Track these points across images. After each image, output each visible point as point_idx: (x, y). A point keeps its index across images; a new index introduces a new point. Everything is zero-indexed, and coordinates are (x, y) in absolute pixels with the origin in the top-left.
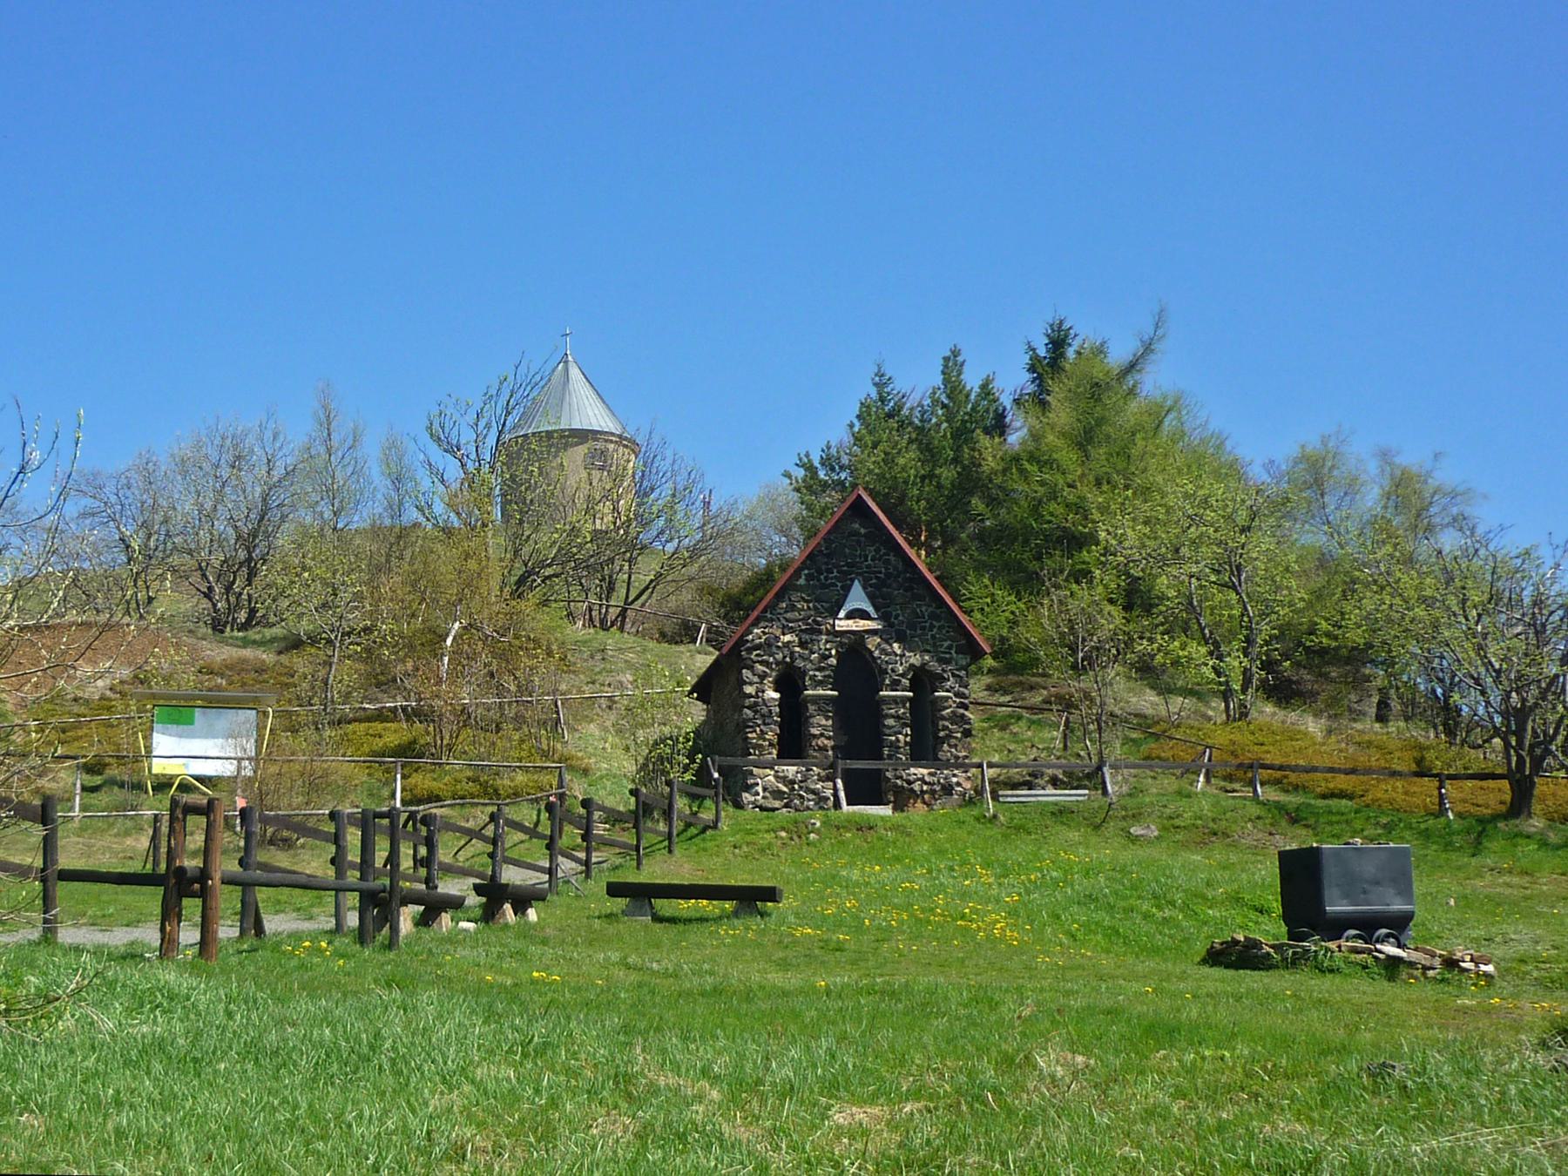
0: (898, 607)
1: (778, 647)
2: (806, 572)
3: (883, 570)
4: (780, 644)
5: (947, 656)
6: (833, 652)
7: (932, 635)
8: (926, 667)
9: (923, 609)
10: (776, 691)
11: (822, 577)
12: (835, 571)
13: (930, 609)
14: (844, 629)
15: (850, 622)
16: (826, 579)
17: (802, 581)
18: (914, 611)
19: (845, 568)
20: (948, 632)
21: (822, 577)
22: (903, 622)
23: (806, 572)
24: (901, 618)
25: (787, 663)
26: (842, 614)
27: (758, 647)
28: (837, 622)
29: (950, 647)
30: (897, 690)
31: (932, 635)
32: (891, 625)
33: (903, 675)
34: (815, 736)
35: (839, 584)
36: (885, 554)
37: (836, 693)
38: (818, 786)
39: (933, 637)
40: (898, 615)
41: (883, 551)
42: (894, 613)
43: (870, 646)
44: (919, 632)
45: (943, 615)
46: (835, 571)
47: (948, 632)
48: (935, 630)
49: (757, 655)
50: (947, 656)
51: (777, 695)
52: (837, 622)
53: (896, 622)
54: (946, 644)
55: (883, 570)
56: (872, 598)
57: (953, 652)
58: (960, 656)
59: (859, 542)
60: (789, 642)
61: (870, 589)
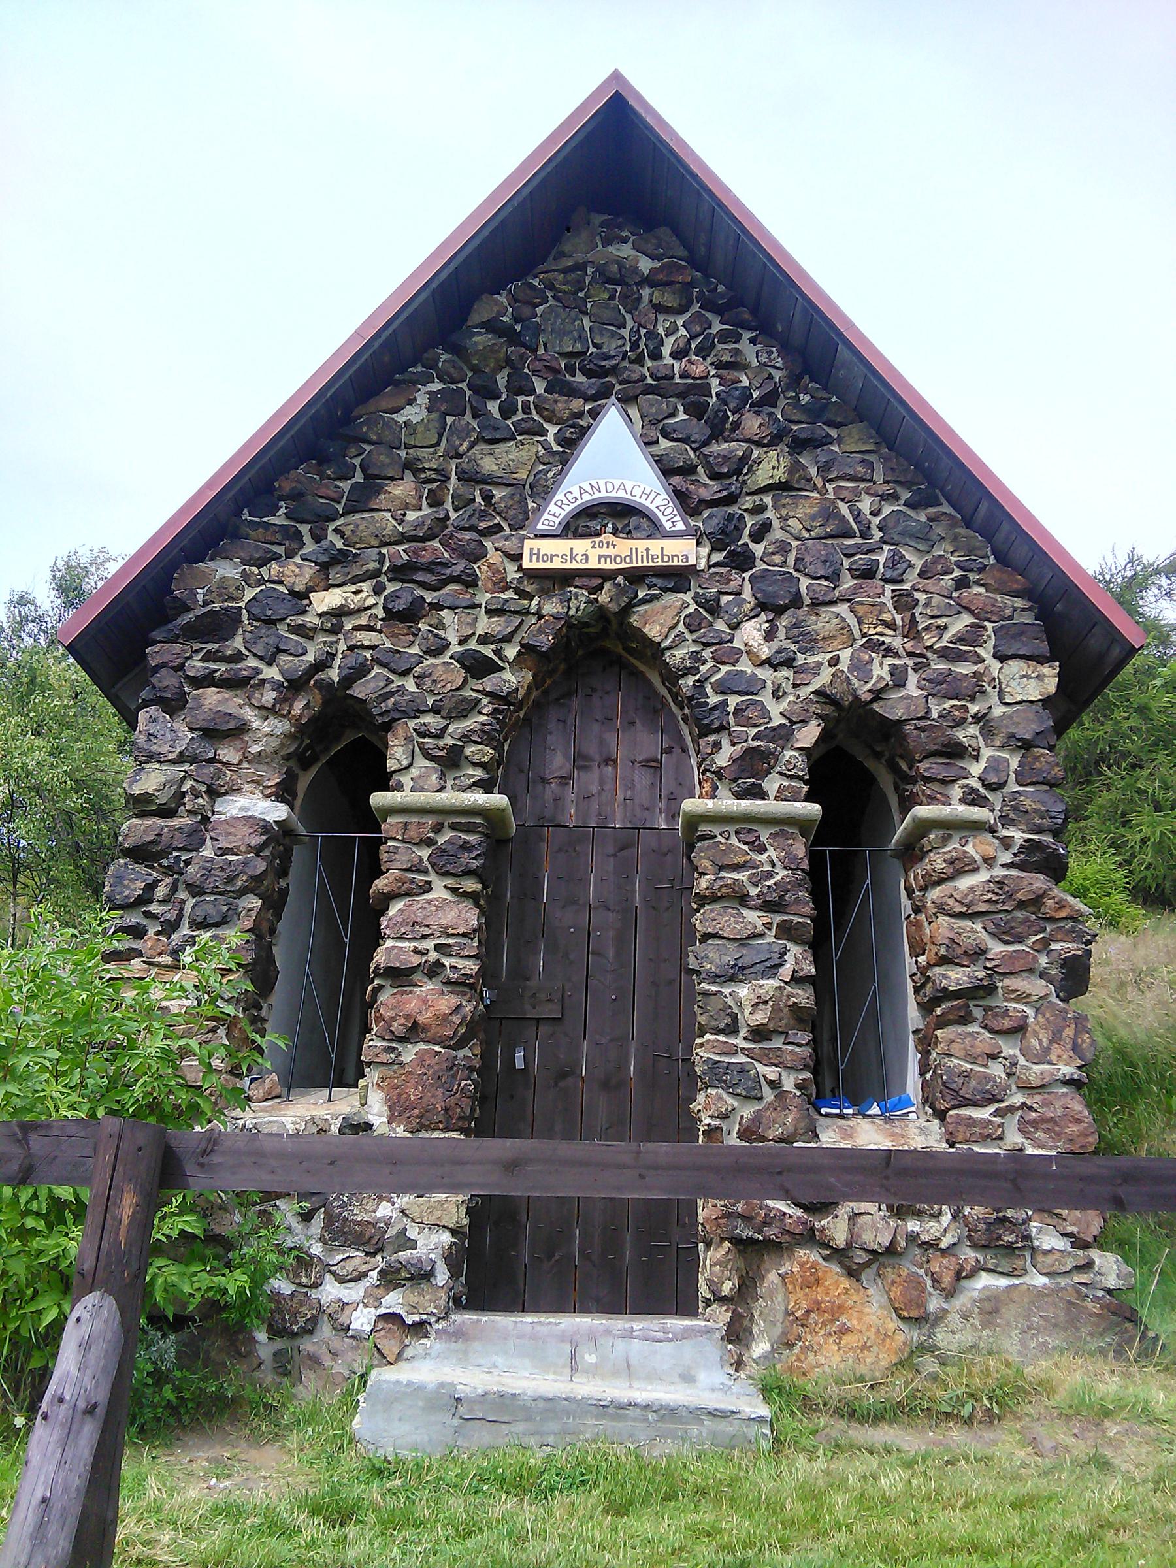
0: (768, 500)
1: (301, 630)
2: (436, 386)
4: (311, 620)
5: (965, 669)
6: (511, 652)
8: (876, 706)
9: (865, 505)
10: (284, 792)
11: (493, 407)
12: (540, 386)
13: (887, 510)
14: (556, 564)
15: (581, 546)
16: (507, 411)
17: (415, 413)
18: (829, 513)
20: (961, 584)
21: (493, 407)
22: (784, 548)
23: (436, 386)
24: (777, 534)
25: (326, 687)
26: (555, 513)
28: (528, 544)
29: (972, 637)
33: (783, 735)
34: (400, 976)
35: (552, 430)
36: (724, 337)
37: (498, 800)
38: (384, 1210)
39: (903, 602)
40: (766, 527)
41: (717, 327)
42: (750, 522)
43: (653, 631)
44: (848, 583)
46: (540, 386)
47: (961, 583)
52: (528, 544)
53: (758, 549)
55: (714, 382)
56: (666, 469)
57: (986, 652)
58: (1015, 667)
59: (632, 303)
60: (340, 613)
61: (665, 444)
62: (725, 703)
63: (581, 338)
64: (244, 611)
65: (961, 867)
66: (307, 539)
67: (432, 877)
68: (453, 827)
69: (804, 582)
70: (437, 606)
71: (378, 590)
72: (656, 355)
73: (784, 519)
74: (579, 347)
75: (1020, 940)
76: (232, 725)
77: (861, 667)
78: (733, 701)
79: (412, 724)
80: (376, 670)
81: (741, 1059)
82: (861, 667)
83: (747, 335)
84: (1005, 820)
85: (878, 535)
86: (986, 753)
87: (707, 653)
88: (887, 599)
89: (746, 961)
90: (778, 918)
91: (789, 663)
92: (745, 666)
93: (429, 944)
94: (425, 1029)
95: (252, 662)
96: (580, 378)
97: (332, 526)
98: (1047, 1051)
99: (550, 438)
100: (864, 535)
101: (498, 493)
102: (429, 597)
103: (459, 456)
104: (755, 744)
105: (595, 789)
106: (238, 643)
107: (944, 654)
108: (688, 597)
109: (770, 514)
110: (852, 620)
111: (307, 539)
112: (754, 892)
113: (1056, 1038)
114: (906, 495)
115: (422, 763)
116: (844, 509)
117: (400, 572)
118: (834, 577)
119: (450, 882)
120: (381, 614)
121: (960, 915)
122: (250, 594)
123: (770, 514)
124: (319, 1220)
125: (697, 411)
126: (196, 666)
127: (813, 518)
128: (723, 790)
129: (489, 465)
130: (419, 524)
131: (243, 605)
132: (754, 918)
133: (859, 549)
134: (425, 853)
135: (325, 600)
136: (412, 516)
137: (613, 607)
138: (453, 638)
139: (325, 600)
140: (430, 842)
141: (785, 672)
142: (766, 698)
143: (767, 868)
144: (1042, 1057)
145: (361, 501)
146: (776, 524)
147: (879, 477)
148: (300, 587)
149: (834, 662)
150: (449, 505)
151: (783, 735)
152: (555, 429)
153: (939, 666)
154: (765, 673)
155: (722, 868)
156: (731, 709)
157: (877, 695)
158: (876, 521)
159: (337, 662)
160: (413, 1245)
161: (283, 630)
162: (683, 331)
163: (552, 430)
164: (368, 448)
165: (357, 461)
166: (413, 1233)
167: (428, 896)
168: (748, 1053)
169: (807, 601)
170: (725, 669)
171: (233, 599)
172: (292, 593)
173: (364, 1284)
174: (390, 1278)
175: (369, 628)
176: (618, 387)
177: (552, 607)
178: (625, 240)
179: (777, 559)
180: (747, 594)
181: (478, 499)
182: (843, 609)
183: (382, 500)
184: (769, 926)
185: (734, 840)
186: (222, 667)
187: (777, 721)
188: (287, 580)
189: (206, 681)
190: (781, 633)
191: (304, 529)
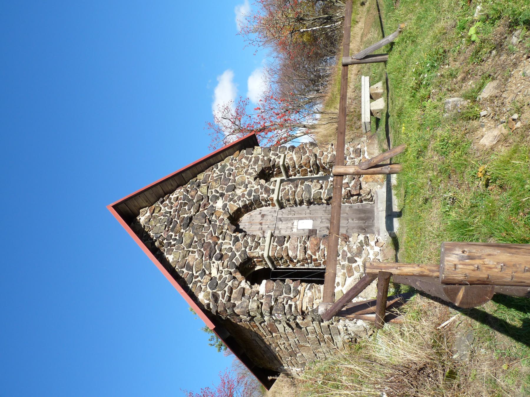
0: (209, 190)
1: (221, 277)
3: (180, 201)
4: (218, 277)
7: (236, 169)
9: (215, 175)
13: (217, 171)
16: (175, 240)
19: (171, 226)
21: (173, 243)
24: (218, 189)
27: (215, 297)
29: (247, 158)
30: (273, 190)
31: (236, 169)
32: (222, 195)
38: (355, 247)
41: (167, 202)
42: (214, 193)
44: (231, 177)
45: (223, 164)
46: (171, 233)
48: (232, 168)
49: (223, 298)
50: (253, 159)
51: (264, 282)
54: (244, 160)
57: (250, 156)
62: (254, 195)
63: (162, 226)
64: (214, 291)
65: (292, 159)
66: (196, 280)
67: (284, 246)
68: (274, 242)
69: (230, 184)
70: (221, 250)
71: (214, 263)
72: (171, 212)
73: (215, 187)
74: (164, 226)
75: (306, 151)
76: (242, 290)
77: (250, 174)
78: (253, 194)
79: (248, 252)
80: (234, 261)
81: (326, 191)
82: (250, 174)
83: (171, 196)
84: (284, 153)
85: (222, 173)
86: (271, 156)
87: (242, 199)
88: (236, 171)
89: (308, 190)
90: (299, 185)
91: (247, 185)
92: (246, 193)
93: (299, 245)
94: (318, 243)
95: (226, 289)
96: (171, 226)
97: (195, 274)
98: (326, 148)
99: (184, 231)
100: (222, 175)
101: (195, 239)
102: (218, 252)
103: (184, 248)
104: (263, 189)
105: (267, 226)
106: (220, 293)
107: (250, 162)
108: (228, 203)
109: (213, 190)
110: (240, 176)
111: (196, 280)
112: (294, 189)
113: (324, 147)
114: (215, 169)
115: (257, 250)
116: (215, 178)
117: (210, 258)
118: (230, 179)
119: (285, 242)
120: (220, 261)
121: (301, 159)
122: (209, 290)
123: (213, 190)
124: (356, 259)
125: (185, 204)
126: (224, 301)
127: (216, 183)
128: (272, 196)
129: (189, 241)
130: (199, 255)
131: (211, 291)
132: (299, 189)
133: (225, 176)
134: (278, 248)
135: (214, 273)
136: (197, 257)
137: (229, 215)
138: (230, 246)
139: (214, 273)
140: (277, 246)
141: (248, 186)
142: (253, 189)
143: (289, 188)
144: (328, 149)
145: (190, 268)
146: (216, 189)
147: (210, 173)
148: (210, 278)
149: (248, 178)
150: (195, 250)
151: (262, 186)
152: (182, 230)
153: (252, 163)
154: (248, 189)
155: (288, 194)
156: (255, 194)
157: (256, 171)
158: (219, 173)
159: (230, 270)
160: (362, 241)
161: (219, 282)
162: (166, 208)
163: (182, 231)
164: (177, 267)
165: (179, 270)
166: (359, 241)
167: (289, 247)
168: (325, 189)
169: (234, 183)
170: (246, 196)
171: (209, 293)
172: (211, 280)
173: (370, 251)
174: (368, 245)
175: (223, 263)
176: (176, 219)
177: (226, 227)
178: (140, 219)
179: (224, 188)
180: (230, 193)
181: (196, 244)
182: (236, 178)
183: (191, 263)
184: (301, 187)
185: (283, 193)
186: (227, 294)
187: (259, 186)
188: (207, 281)
189: (229, 300)
190: (240, 187)
191: (194, 280)
